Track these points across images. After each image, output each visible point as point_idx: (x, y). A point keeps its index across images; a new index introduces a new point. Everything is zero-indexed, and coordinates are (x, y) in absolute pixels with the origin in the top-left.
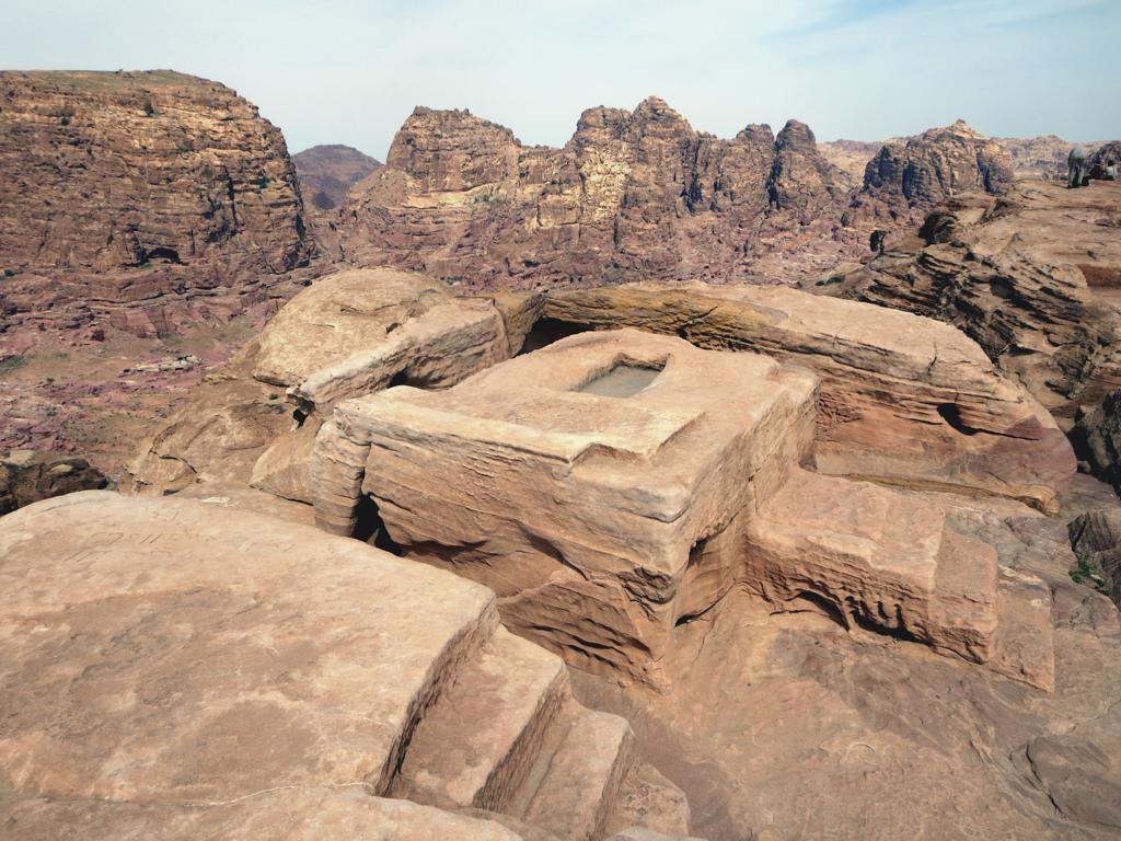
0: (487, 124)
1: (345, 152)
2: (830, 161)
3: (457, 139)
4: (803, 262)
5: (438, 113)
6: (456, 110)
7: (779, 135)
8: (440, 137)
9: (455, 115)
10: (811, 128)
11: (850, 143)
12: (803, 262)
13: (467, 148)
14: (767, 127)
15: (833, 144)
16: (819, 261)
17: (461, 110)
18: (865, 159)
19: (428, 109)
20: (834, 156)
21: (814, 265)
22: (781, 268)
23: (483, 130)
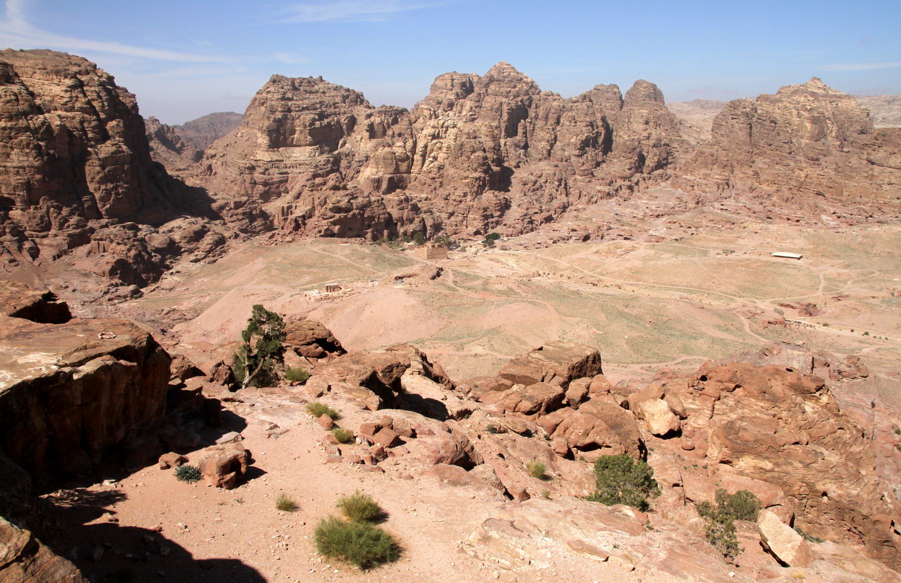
0: (336, 89)
1: (234, 118)
2: (680, 116)
3: (306, 101)
4: (636, 207)
5: (293, 81)
6: (311, 77)
7: (627, 93)
8: (291, 99)
9: (310, 82)
10: (659, 87)
11: (707, 102)
12: (636, 207)
13: (315, 109)
14: (616, 86)
15: (689, 103)
16: (654, 207)
17: (316, 77)
18: (711, 115)
19: (283, 77)
20: (688, 113)
21: (647, 211)
22: (612, 215)
23: (334, 93)
